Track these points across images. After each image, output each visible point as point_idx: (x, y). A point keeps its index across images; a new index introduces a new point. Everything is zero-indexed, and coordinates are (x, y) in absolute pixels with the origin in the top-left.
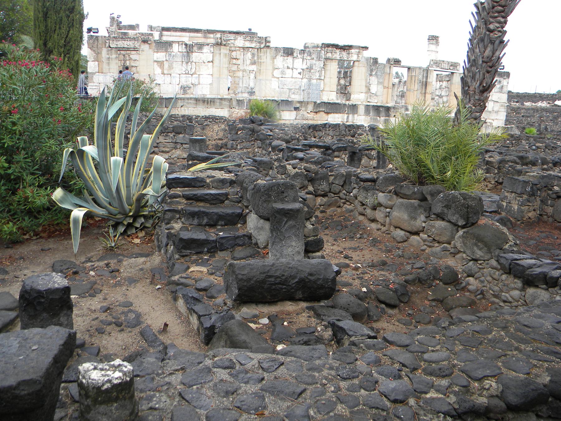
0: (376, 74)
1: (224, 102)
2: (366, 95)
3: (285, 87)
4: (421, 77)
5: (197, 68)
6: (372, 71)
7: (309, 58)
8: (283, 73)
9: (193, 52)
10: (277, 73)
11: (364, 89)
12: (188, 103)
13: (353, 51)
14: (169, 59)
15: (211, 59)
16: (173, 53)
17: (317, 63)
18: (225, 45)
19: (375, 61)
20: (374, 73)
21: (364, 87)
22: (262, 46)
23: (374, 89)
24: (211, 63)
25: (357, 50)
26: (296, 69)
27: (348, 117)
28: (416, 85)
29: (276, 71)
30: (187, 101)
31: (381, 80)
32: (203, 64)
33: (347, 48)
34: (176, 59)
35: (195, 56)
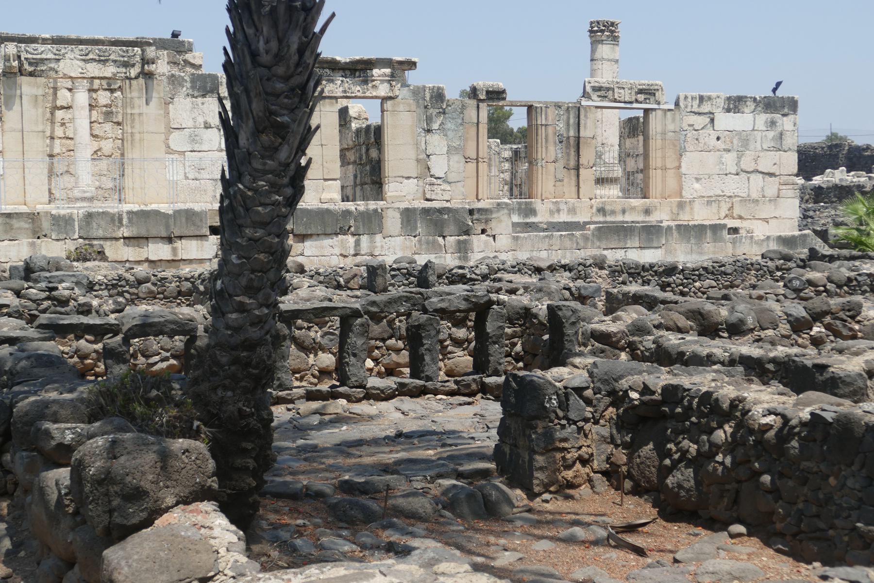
1: (16, 223)
2: (421, 183)
3: (205, 175)
4: (561, 125)
6: (429, 120)
8: (193, 139)
10: (177, 141)
11: (412, 169)
13: (376, 72)
18: (31, 74)
19: (438, 96)
20: (435, 126)
22: (133, 72)
23: (439, 166)
25: (388, 71)
27: (357, 244)
28: (551, 148)
29: (175, 136)
33: (359, 67)
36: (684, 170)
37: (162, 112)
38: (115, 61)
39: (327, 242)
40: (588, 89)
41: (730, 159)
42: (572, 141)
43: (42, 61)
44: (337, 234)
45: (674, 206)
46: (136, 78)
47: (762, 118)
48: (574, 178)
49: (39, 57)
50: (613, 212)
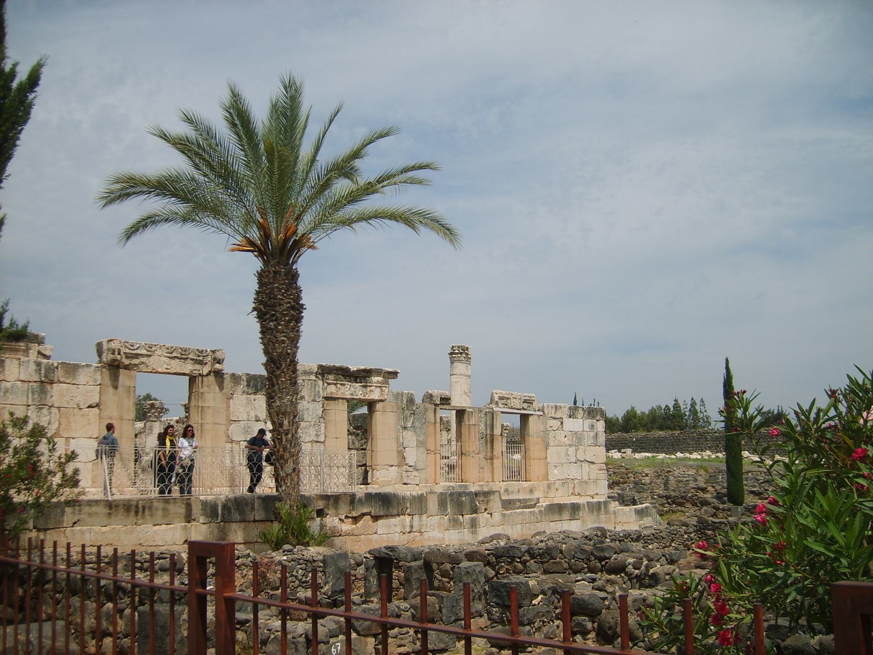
0: (413, 426)
5: (63, 421)
9: (52, 383)
11: (394, 459)
12: (90, 514)
15: (96, 400)
17: (311, 406)
21: (395, 454)
22: (206, 370)
23: (412, 456)
24: (96, 409)
25: (380, 379)
27: (411, 521)
29: (233, 427)
36: (548, 460)
37: (225, 406)
38: (193, 360)
39: (392, 521)
40: (496, 399)
41: (571, 450)
42: (488, 436)
43: (137, 356)
44: (399, 515)
45: (546, 486)
46: (207, 375)
47: (588, 422)
48: (490, 466)
49: (135, 352)
50: (512, 492)
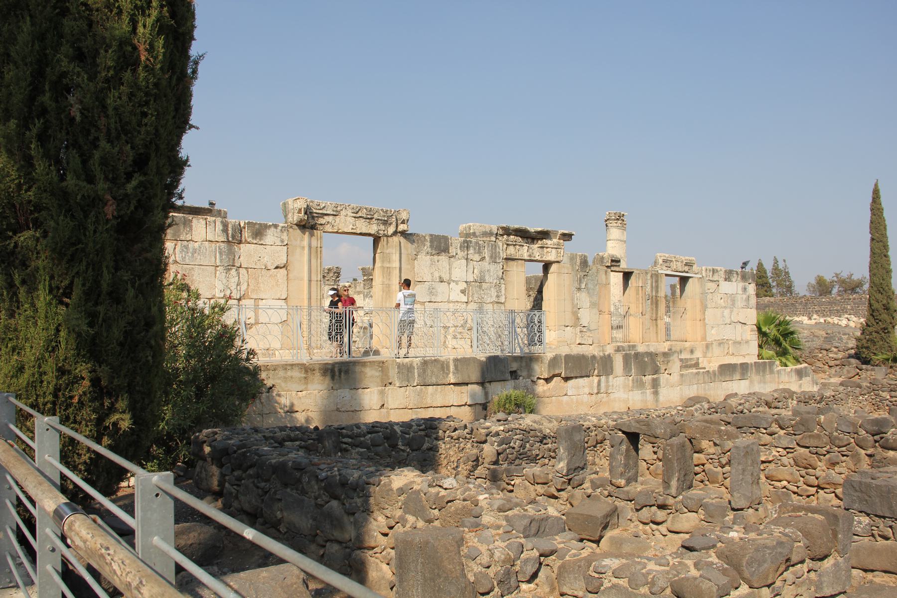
5: (252, 282)
7: (477, 257)
9: (240, 242)
12: (285, 379)
14: (184, 258)
16: (191, 245)
17: (493, 267)
22: (391, 230)
26: (457, 282)
30: (281, 373)
31: (595, 299)
32: (264, 272)
34: (199, 259)
35: (247, 252)
